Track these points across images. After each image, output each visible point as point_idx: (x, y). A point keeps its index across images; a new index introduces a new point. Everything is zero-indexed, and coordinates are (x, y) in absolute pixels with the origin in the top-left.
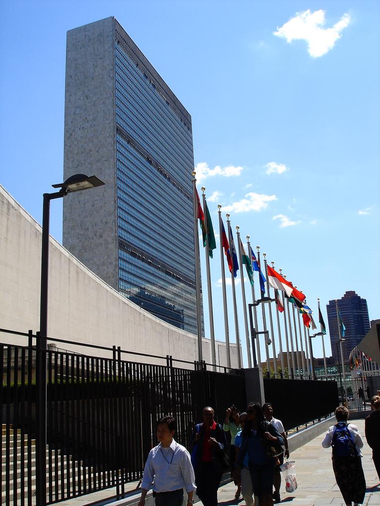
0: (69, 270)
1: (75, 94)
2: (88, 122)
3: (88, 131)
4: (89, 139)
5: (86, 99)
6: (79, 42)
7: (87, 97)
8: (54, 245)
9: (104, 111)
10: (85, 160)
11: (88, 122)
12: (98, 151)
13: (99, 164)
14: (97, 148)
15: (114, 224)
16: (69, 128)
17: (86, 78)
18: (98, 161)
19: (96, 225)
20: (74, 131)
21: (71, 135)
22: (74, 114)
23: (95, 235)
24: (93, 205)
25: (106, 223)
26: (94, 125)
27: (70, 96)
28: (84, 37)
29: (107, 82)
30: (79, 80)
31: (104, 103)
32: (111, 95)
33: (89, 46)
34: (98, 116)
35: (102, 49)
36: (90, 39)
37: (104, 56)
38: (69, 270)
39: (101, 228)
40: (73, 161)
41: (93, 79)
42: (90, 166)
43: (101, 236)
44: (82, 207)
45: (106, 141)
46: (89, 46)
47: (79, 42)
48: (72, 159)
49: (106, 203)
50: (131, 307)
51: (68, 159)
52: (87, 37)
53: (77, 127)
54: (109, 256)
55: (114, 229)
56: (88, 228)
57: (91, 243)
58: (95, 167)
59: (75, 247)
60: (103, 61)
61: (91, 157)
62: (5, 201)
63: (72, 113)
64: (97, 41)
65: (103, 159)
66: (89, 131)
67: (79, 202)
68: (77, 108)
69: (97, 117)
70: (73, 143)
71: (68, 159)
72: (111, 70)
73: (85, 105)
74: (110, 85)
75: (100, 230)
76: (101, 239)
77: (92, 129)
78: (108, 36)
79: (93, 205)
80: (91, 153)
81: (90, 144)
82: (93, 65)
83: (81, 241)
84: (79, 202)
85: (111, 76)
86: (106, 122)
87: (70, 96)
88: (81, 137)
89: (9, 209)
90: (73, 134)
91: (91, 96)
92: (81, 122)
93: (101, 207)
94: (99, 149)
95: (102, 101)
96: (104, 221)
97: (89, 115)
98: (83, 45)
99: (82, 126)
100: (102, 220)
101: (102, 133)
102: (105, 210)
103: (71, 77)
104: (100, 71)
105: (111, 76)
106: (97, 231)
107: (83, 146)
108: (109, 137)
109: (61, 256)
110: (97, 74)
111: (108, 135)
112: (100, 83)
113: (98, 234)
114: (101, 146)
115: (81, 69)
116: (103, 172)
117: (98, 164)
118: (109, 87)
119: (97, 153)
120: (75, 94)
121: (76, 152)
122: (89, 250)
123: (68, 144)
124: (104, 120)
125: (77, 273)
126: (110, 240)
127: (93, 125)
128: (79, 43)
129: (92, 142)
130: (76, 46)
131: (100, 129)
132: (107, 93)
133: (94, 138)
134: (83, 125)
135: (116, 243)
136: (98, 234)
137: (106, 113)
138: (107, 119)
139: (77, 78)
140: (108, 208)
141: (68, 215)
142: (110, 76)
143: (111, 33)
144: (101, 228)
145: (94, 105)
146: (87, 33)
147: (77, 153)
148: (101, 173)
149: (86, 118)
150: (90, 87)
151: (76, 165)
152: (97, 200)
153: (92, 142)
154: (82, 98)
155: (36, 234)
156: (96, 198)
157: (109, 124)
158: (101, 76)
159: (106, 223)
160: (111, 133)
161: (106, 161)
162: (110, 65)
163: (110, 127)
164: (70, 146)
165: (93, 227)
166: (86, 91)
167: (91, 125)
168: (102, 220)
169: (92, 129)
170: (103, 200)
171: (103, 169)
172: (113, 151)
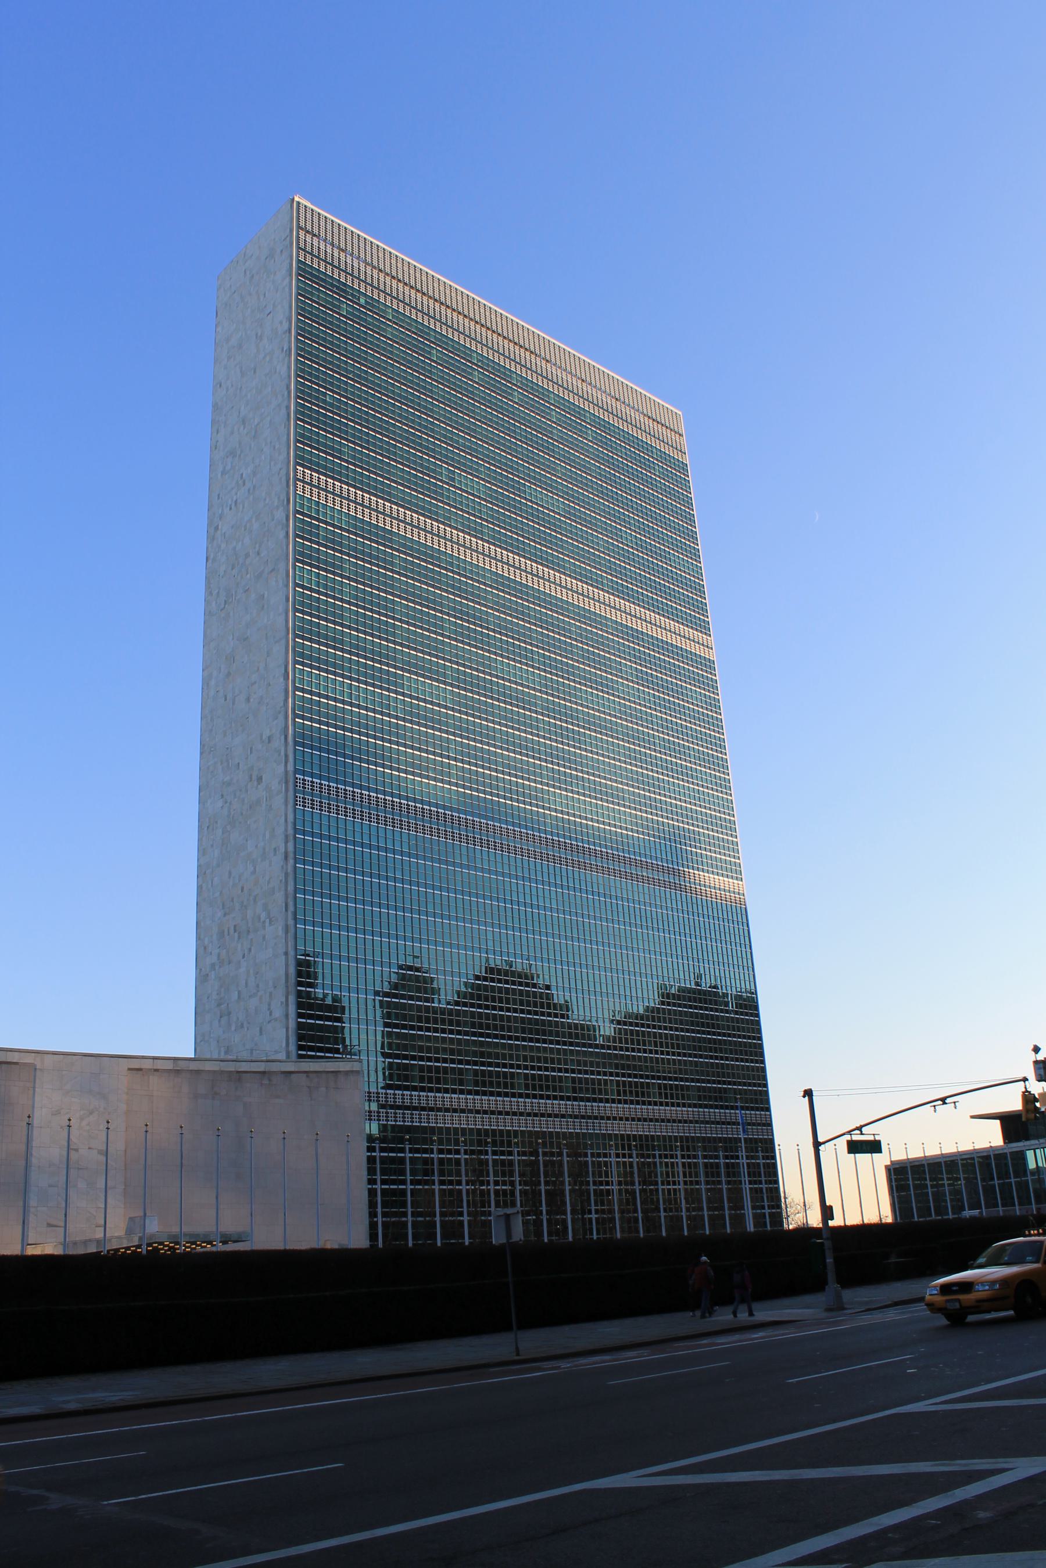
2: (244, 484)
5: (242, 426)
6: (235, 292)
7: (244, 422)
9: (271, 443)
12: (258, 554)
14: (257, 546)
15: (283, 737)
21: (217, 528)
24: (248, 700)
26: (254, 487)
32: (283, 395)
36: (253, 276)
41: (255, 372)
43: (260, 779)
47: (235, 292)
51: (211, 594)
52: (248, 273)
54: (274, 830)
57: (243, 800)
58: (253, 596)
59: (217, 822)
61: (247, 574)
67: (226, 700)
68: (227, 457)
70: (219, 547)
76: (259, 786)
78: (282, 251)
79: (248, 700)
82: (257, 335)
83: (226, 802)
84: (226, 700)
88: (232, 527)
90: (220, 527)
92: (233, 489)
93: (262, 697)
94: (260, 546)
95: (268, 419)
96: (267, 733)
99: (235, 499)
101: (267, 500)
102: (268, 704)
103: (220, 386)
104: (267, 347)
106: (251, 768)
107: (234, 548)
108: (277, 508)
116: (265, 607)
122: (240, 823)
123: (212, 557)
128: (235, 294)
133: (254, 520)
134: (236, 494)
141: (208, 739)
149: (242, 474)
152: (255, 683)
158: (268, 359)
159: (270, 739)
161: (271, 571)
163: (281, 479)
164: (214, 560)
167: (249, 490)
169: (251, 498)
171: (266, 593)
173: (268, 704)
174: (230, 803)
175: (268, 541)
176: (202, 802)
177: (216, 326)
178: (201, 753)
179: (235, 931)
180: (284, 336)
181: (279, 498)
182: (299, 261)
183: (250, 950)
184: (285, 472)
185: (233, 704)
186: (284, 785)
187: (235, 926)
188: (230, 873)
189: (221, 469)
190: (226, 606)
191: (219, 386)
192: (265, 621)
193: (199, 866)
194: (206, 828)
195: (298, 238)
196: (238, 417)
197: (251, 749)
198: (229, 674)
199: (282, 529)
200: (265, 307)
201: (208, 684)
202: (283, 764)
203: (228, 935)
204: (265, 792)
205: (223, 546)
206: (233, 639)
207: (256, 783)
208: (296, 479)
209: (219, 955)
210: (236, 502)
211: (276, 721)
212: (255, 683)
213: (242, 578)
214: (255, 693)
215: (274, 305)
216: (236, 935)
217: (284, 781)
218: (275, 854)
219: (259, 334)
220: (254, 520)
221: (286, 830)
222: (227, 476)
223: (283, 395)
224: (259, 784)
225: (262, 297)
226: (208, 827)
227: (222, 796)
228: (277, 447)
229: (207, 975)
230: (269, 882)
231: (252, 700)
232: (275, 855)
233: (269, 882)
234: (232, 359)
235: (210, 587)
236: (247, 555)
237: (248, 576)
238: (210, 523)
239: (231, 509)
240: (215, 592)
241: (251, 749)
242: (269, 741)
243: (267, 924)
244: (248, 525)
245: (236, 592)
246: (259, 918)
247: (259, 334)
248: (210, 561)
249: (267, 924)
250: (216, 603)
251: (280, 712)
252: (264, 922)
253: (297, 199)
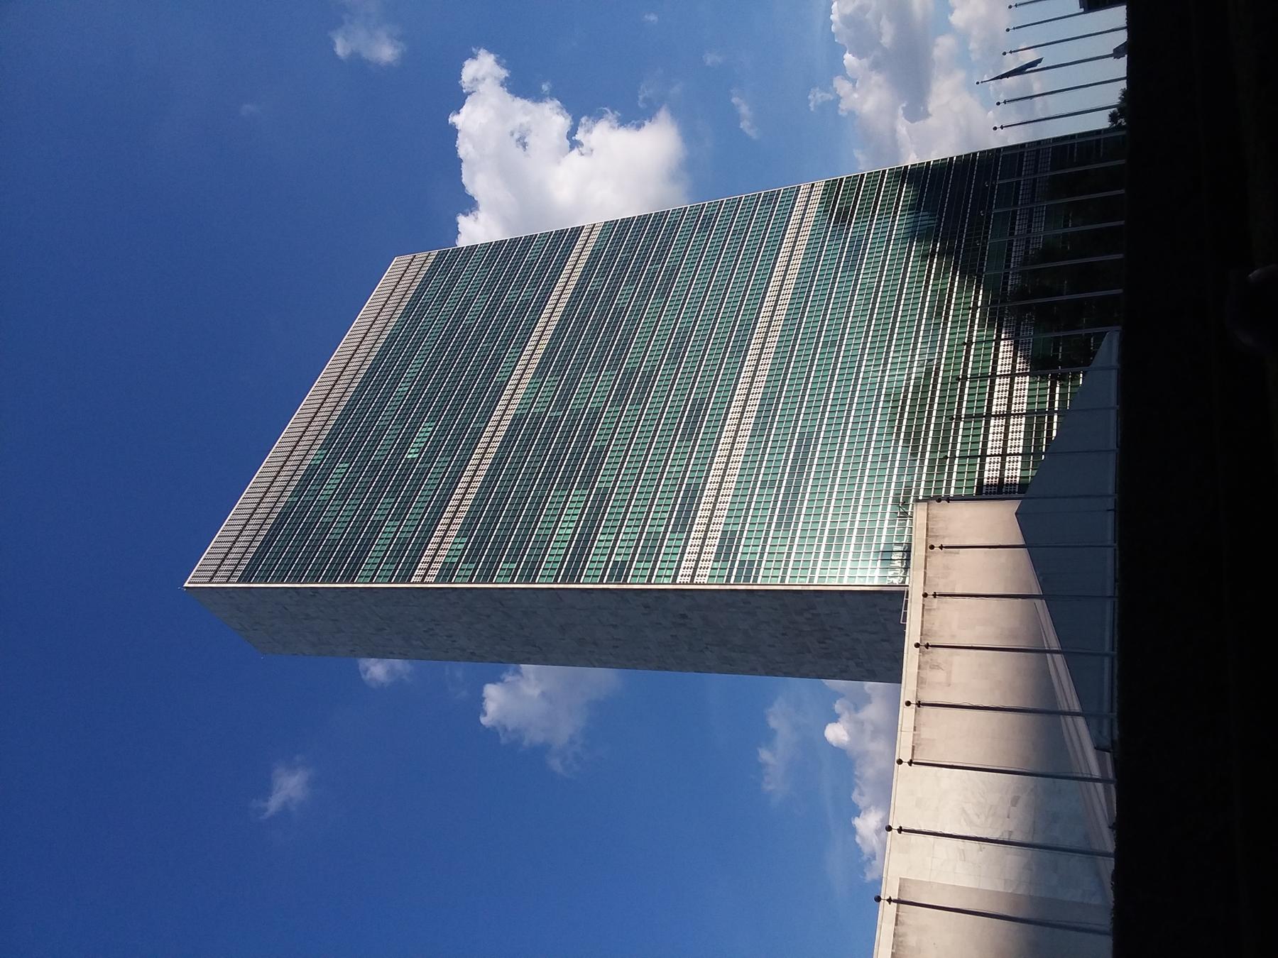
2: (433, 629)
4: (470, 628)
12: (488, 616)
15: (644, 595)
24: (615, 626)
25: (646, 607)
27: (392, 653)
41: (336, 620)
43: (684, 616)
52: (255, 628)
67: (617, 647)
76: (689, 617)
79: (615, 626)
83: (707, 648)
84: (617, 647)
88: (469, 640)
90: (472, 651)
99: (445, 638)
133: (461, 620)
149: (424, 631)
159: (646, 607)
161: (502, 605)
167: (436, 625)
168: (644, 614)
174: (707, 644)
176: (709, 670)
177: (304, 654)
178: (666, 670)
179: (824, 643)
182: (238, 582)
183: (841, 629)
185: (620, 640)
187: (820, 642)
188: (769, 646)
193: (767, 674)
194: (732, 667)
195: (218, 583)
197: (657, 624)
203: (826, 649)
206: (564, 639)
208: (422, 582)
209: (848, 659)
216: (827, 641)
218: (750, 603)
220: (461, 620)
224: (687, 617)
226: (731, 665)
227: (702, 651)
229: (867, 670)
230: (776, 609)
231: (614, 623)
232: (750, 603)
233: (776, 609)
238: (469, 659)
241: (657, 624)
242: (649, 607)
243: (814, 612)
246: (808, 619)
248: (502, 660)
249: (814, 612)
252: (813, 614)
253: (186, 585)
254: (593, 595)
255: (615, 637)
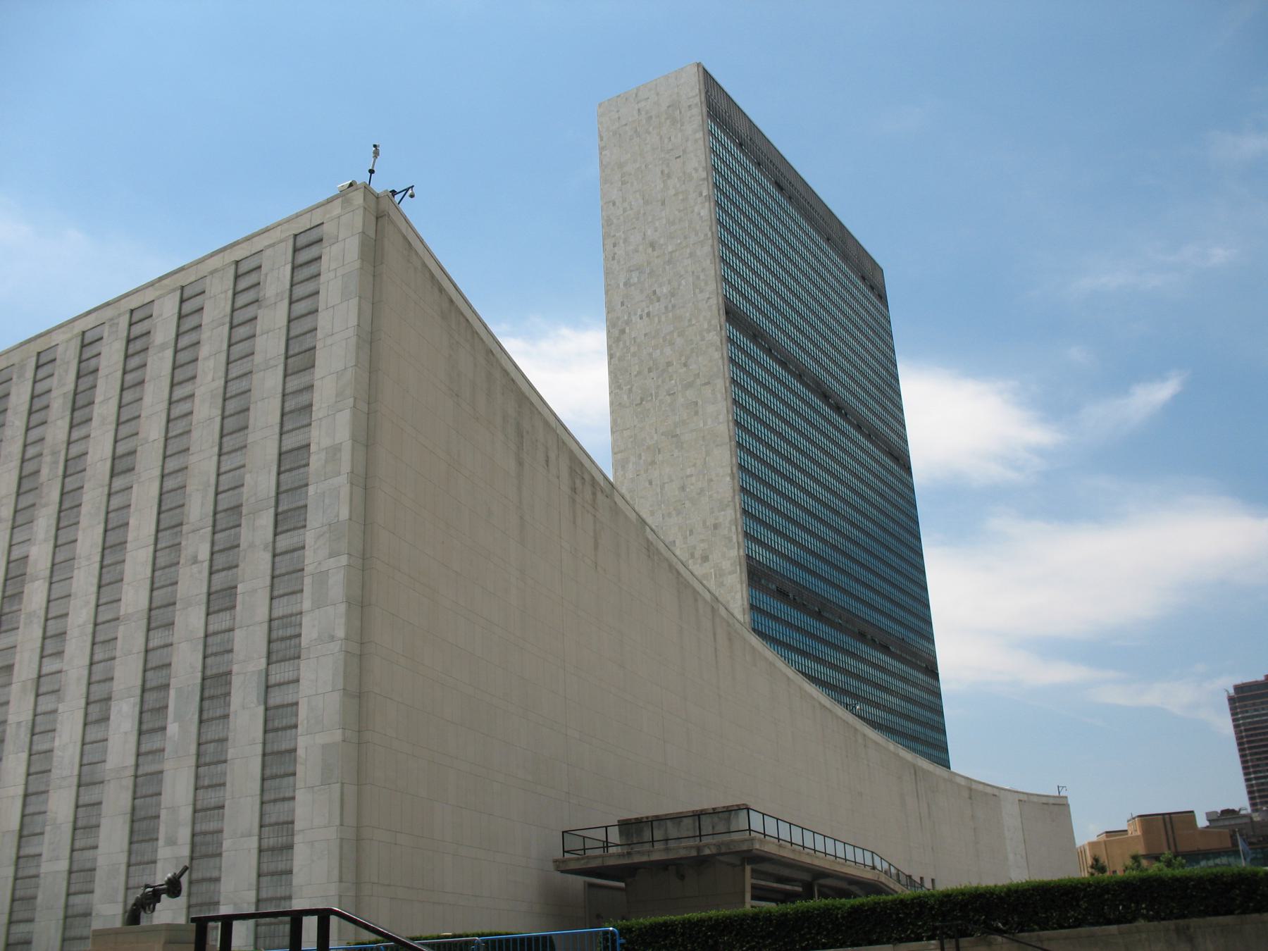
0: (715, 634)
1: (625, 241)
2: (658, 301)
3: (659, 322)
4: (664, 340)
5: (651, 249)
6: (626, 125)
7: (653, 245)
8: (682, 576)
9: (693, 272)
10: (658, 387)
11: (658, 300)
13: (690, 393)
14: (683, 358)
15: (734, 528)
16: (618, 318)
17: (646, 203)
18: (690, 385)
19: (691, 532)
20: (628, 322)
21: (623, 331)
22: (625, 284)
23: (692, 556)
24: (683, 488)
25: (716, 527)
26: (674, 306)
27: (615, 245)
28: (635, 113)
29: (696, 210)
30: (632, 209)
31: (692, 255)
32: (706, 235)
33: (649, 133)
34: (680, 285)
35: (680, 135)
36: (651, 117)
37: (684, 151)
38: (715, 634)
39: (703, 541)
40: (630, 390)
41: (663, 203)
42: (668, 399)
43: (705, 559)
44: (657, 494)
45: (703, 340)
46: (649, 133)
47: (626, 125)
48: (629, 387)
49: (711, 480)
50: (838, 717)
52: (643, 113)
53: (635, 314)
55: (735, 540)
56: (674, 541)
58: (681, 400)
60: (684, 163)
61: (671, 380)
62: (587, 477)
63: (621, 285)
64: (667, 119)
65: (698, 382)
66: (663, 319)
67: (651, 483)
68: (631, 271)
69: (679, 288)
71: (620, 387)
72: (704, 179)
73: (649, 263)
74: (702, 214)
75: (702, 545)
77: (670, 314)
78: (690, 106)
79: (683, 488)
80: (670, 369)
81: (668, 351)
82: (662, 172)
84: (651, 483)
85: (704, 194)
86: (700, 296)
87: (615, 245)
88: (645, 335)
89: (594, 494)
90: (627, 331)
91: (662, 241)
92: (642, 301)
93: (702, 490)
95: (688, 251)
96: (710, 522)
97: (661, 286)
98: (636, 131)
99: (646, 311)
100: (704, 522)
101: (694, 322)
103: (614, 204)
104: (678, 186)
105: (704, 194)
106: (694, 547)
107: (650, 355)
108: (709, 331)
109: (696, 600)
110: (672, 192)
111: (706, 326)
112: (680, 211)
113: (698, 553)
114: (692, 351)
115: (635, 183)
116: (700, 413)
117: (688, 393)
118: (701, 217)
119: (685, 369)
120: (625, 241)
121: (635, 369)
123: (618, 354)
124: (694, 293)
125: (730, 640)
126: (726, 565)
127: (670, 306)
128: (627, 128)
129: (672, 344)
130: (620, 135)
131: (688, 315)
132: (697, 234)
133: (675, 334)
134: (648, 307)
135: (741, 572)
136: (698, 553)
137: (698, 278)
138: (701, 291)
139: (626, 205)
140: (718, 492)
142: (701, 194)
143: (697, 100)
144: (703, 541)
145: (669, 262)
146: (642, 104)
147: (639, 373)
148: (696, 413)
149: (655, 292)
150: (657, 224)
151: (639, 398)
152: (691, 476)
153: (672, 344)
154: (641, 248)
155: (648, 550)
156: (688, 471)
157: (707, 302)
158: (681, 197)
159: (716, 527)
160: (713, 322)
162: (701, 169)
163: (710, 307)
164: (621, 359)
165: (685, 538)
166: (649, 232)
167: (666, 308)
168: (704, 522)
169: (670, 314)
170: (704, 475)
171: (700, 403)
172: (720, 362)
173: (710, 497)
175: (698, 357)
180: (701, 183)
181: (709, 322)
184: (715, 302)
185: (662, 488)
186: (738, 567)
189: (623, 280)
190: (644, 403)
191: (611, 204)
192: (702, 425)
196: (644, 239)
198: (653, 463)
199: (716, 350)
200: (672, 150)
201: (623, 467)
202: (736, 553)
204: (712, 570)
205: (632, 349)
206: (656, 433)
207: (699, 561)
210: (648, 314)
211: (723, 513)
212: (691, 476)
213: (663, 382)
214: (692, 484)
215: (684, 151)
217: (738, 563)
219: (666, 172)
221: (743, 605)
222: (633, 287)
223: (706, 235)
224: (705, 562)
225: (666, 141)
228: (702, 277)
234: (629, 185)
235: (618, 382)
236: (669, 364)
237: (673, 382)
239: (641, 318)
240: (626, 388)
244: (668, 337)
245: (657, 394)
247: (666, 172)
250: (629, 397)
251: (727, 506)
254: (728, 479)
255: (666, 485)
